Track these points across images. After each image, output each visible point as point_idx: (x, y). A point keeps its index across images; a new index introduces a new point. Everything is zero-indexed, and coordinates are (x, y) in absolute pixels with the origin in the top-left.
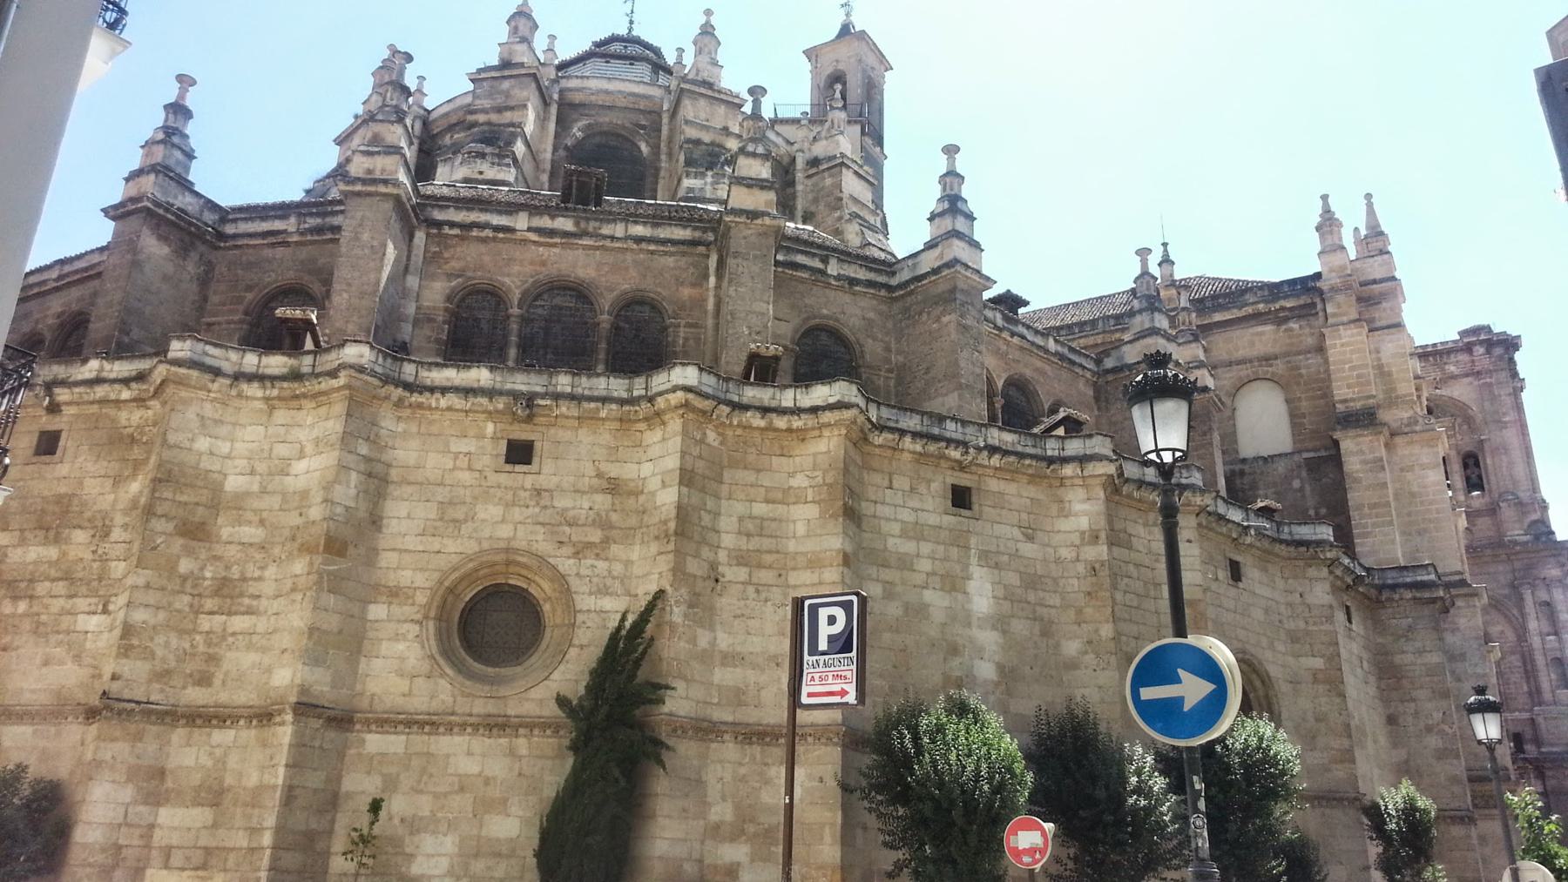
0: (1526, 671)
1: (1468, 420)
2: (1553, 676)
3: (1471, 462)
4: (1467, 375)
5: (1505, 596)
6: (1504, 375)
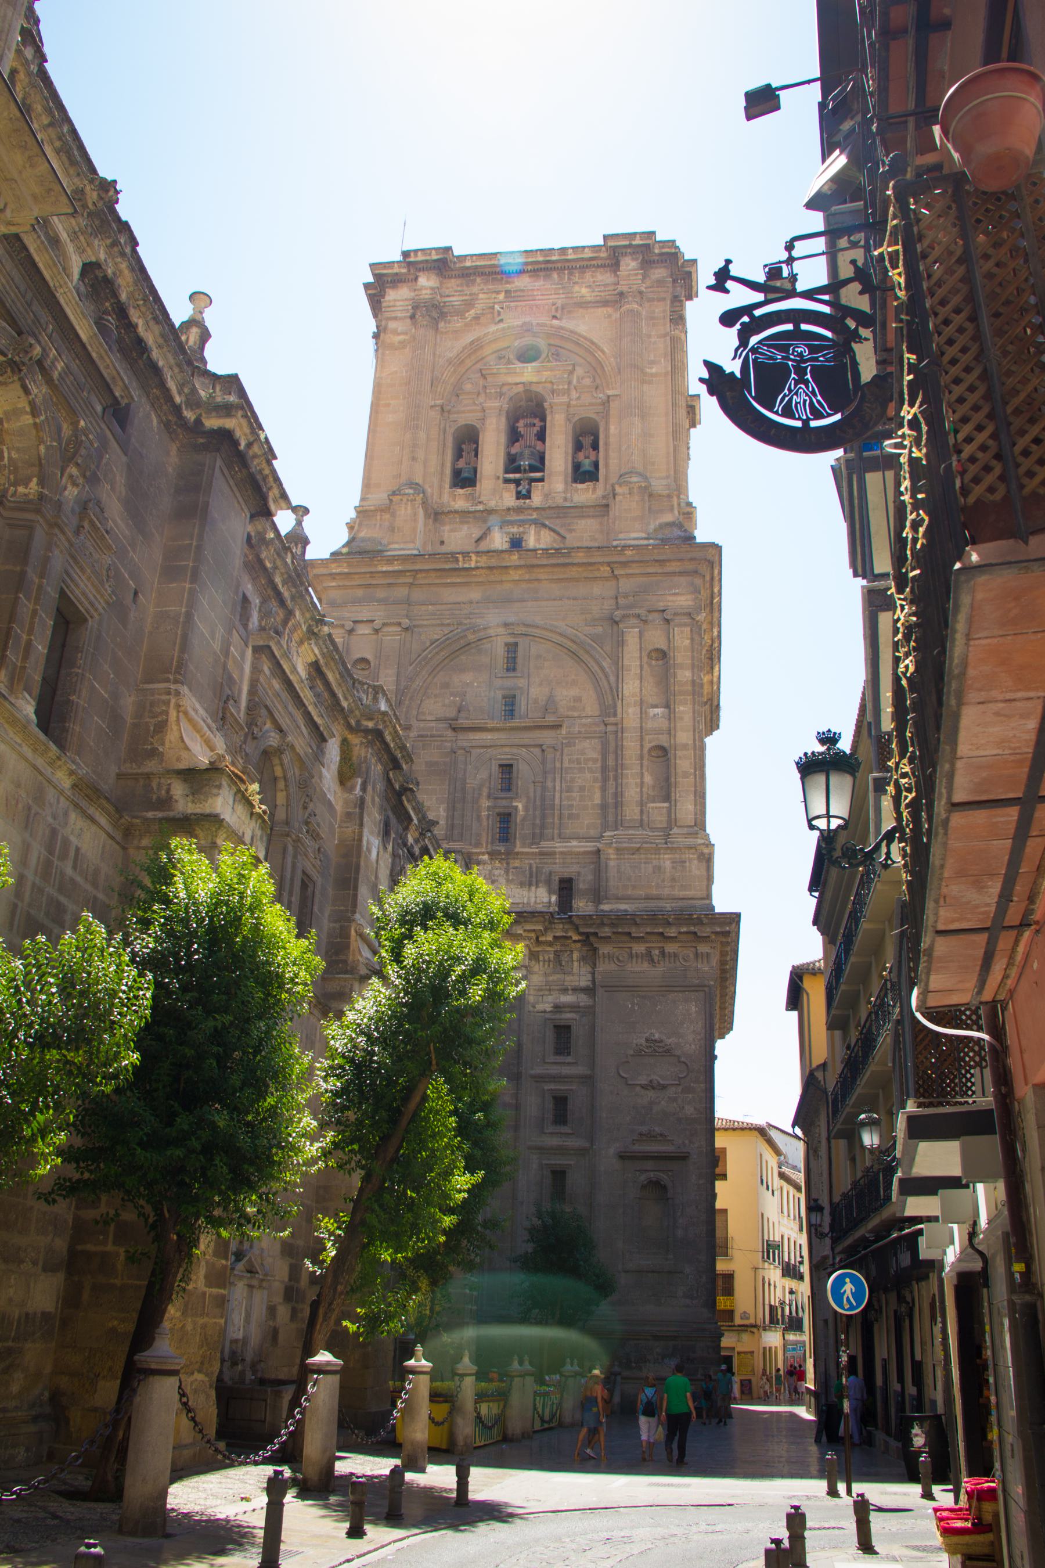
0: (604, 769)
1: (596, 369)
2: (648, 779)
3: (587, 441)
4: (605, 303)
5: (595, 638)
6: (662, 309)
